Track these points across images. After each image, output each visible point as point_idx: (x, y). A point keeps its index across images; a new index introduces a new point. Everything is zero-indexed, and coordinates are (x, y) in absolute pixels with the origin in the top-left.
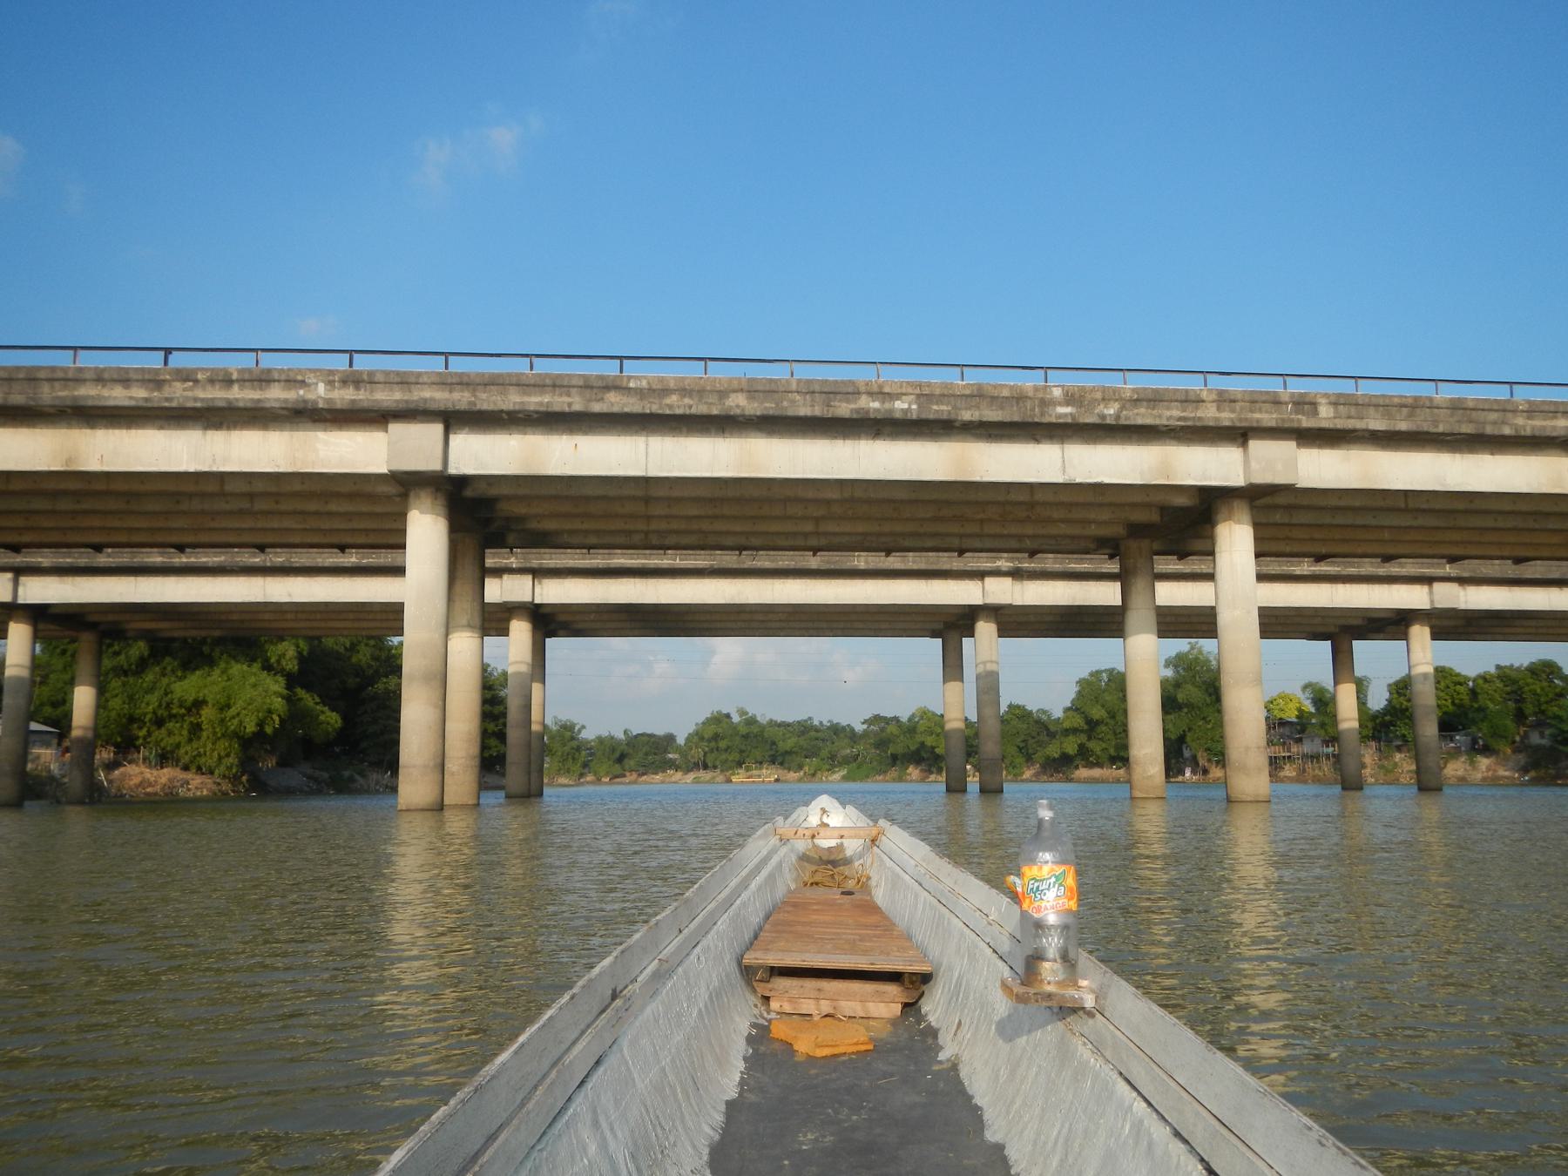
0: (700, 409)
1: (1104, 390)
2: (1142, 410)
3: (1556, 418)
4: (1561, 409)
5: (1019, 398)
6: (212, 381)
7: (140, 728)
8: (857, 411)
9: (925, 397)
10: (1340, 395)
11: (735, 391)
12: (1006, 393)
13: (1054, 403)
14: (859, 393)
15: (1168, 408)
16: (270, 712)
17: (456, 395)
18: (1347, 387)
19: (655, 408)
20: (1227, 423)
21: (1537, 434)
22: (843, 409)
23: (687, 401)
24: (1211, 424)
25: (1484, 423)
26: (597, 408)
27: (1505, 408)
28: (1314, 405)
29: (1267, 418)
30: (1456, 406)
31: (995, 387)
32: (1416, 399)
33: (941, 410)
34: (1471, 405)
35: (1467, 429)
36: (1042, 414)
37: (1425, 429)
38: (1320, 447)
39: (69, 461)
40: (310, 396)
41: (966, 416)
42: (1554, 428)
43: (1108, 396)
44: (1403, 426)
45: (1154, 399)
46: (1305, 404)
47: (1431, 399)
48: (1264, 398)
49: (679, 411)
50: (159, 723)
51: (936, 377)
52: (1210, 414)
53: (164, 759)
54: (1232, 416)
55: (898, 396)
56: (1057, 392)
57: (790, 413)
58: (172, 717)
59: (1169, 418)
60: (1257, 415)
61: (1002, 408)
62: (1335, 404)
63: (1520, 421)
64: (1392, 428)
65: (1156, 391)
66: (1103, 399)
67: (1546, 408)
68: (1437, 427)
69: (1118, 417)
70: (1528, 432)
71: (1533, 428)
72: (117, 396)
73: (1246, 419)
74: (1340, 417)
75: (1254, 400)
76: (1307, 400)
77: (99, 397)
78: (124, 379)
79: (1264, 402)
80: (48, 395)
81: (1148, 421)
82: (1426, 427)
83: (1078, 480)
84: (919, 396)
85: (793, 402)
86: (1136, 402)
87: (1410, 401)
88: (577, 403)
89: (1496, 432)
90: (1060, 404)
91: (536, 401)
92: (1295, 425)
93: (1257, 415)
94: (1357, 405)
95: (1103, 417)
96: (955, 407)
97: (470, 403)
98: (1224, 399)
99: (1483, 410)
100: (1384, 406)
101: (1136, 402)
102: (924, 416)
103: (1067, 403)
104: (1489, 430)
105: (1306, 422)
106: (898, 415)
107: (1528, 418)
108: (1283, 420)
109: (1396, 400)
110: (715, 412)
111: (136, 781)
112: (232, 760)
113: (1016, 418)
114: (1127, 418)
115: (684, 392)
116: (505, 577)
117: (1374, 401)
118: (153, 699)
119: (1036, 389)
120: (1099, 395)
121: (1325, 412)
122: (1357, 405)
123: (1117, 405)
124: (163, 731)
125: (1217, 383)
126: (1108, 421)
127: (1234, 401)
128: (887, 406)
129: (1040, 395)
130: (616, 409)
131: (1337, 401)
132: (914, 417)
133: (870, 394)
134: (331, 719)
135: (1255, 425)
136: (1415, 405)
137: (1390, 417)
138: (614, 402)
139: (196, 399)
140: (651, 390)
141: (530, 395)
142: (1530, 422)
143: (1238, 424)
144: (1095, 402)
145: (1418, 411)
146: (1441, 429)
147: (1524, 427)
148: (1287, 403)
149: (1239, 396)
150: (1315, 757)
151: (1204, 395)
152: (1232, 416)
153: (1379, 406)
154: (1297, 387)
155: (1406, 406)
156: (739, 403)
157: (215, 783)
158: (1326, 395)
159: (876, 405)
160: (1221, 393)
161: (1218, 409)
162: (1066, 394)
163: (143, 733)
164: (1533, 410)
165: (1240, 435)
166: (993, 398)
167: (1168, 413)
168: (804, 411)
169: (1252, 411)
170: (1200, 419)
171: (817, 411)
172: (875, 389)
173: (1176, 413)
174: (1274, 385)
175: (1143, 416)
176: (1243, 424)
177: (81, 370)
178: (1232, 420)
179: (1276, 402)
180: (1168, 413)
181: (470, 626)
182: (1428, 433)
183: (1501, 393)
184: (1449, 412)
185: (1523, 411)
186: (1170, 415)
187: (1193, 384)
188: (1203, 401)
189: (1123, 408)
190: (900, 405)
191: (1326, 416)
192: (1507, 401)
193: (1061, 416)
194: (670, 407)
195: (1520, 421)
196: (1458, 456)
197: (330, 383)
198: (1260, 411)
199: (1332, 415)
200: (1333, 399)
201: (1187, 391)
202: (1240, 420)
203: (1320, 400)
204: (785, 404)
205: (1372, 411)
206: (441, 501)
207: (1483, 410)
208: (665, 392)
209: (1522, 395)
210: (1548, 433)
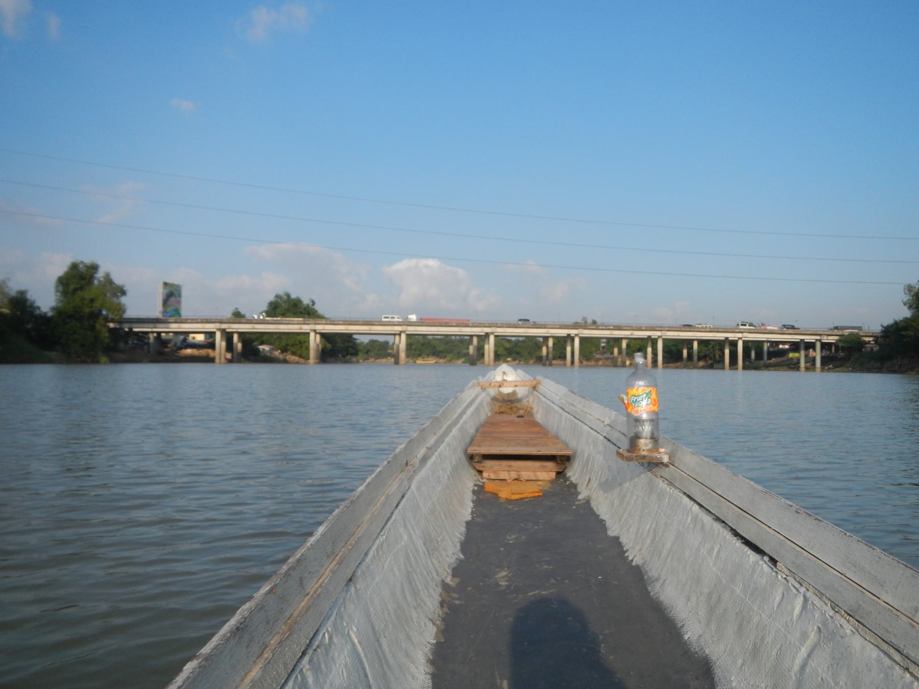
22: (448, 325)
29: (492, 325)
43: (475, 323)
45: (480, 324)
46: (497, 324)
50: (293, 345)
52: (487, 325)
53: (294, 354)
58: (296, 344)
72: (376, 323)
78: (377, 322)
98: (488, 323)
124: (292, 348)
134: (329, 346)
138: (425, 324)
150: (607, 359)
165: (490, 327)
186: (482, 325)
187: (484, 322)
191: (499, 325)
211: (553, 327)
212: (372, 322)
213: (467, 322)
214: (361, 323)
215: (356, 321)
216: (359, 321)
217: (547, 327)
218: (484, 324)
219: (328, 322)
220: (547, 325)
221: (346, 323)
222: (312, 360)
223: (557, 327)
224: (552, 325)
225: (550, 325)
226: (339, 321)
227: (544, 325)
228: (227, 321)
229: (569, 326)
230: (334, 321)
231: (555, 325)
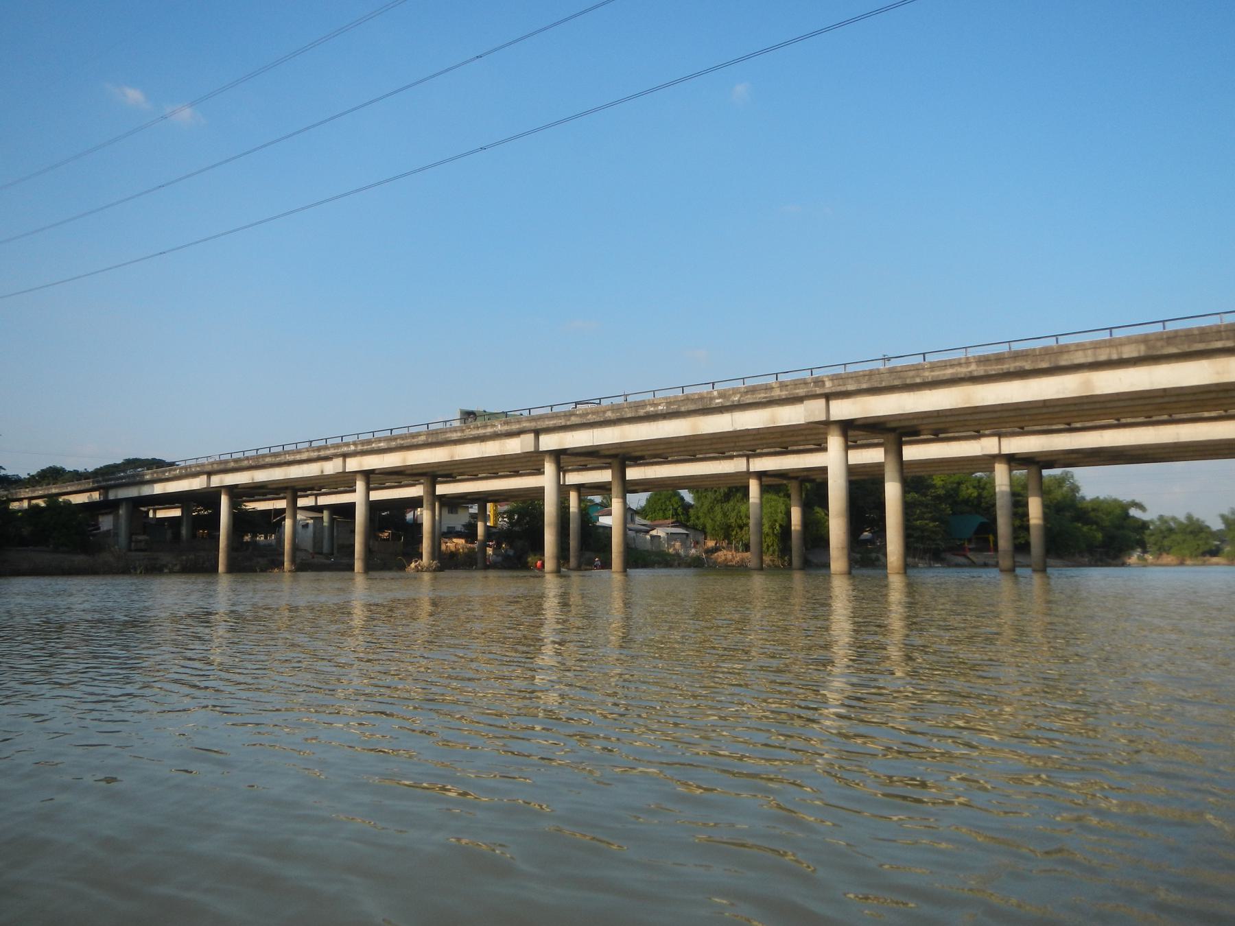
0: (598, 419)
1: (733, 389)
2: (749, 396)
3: (946, 369)
4: (948, 364)
5: (701, 398)
6: (474, 428)
7: (733, 531)
8: (645, 413)
9: (669, 404)
10: (834, 375)
11: (608, 410)
12: (696, 397)
13: (715, 398)
14: (646, 405)
15: (760, 394)
16: (776, 521)
17: (532, 424)
18: (841, 370)
19: (585, 421)
20: (784, 397)
21: (935, 379)
22: (642, 412)
23: (594, 416)
24: (777, 398)
25: (907, 378)
26: (568, 423)
27: (917, 368)
28: (823, 382)
29: (801, 391)
30: (892, 371)
31: (692, 394)
32: (871, 371)
33: (674, 407)
34: (899, 369)
35: (897, 382)
36: (710, 404)
37: (876, 386)
38: (842, 399)
39: (452, 457)
40: (497, 430)
41: (683, 409)
42: (944, 374)
43: (735, 391)
44: (864, 386)
45: (753, 390)
46: (819, 382)
47: (878, 369)
48: (799, 382)
49: (592, 421)
50: (741, 528)
51: (670, 394)
52: (777, 393)
54: (787, 393)
55: (659, 404)
56: (715, 393)
57: (625, 416)
59: (760, 398)
60: (797, 391)
61: (695, 404)
62: (832, 380)
63: (927, 374)
64: (858, 388)
65: (754, 386)
66: (733, 394)
67: (939, 364)
68: (882, 384)
69: (739, 401)
70: (930, 379)
71: (933, 376)
73: (793, 394)
74: (835, 386)
75: (796, 384)
76: (820, 379)
77: (451, 437)
79: (800, 384)
80: (441, 437)
81: (751, 401)
82: (876, 385)
83: (738, 429)
84: (667, 403)
85: (626, 412)
86: (747, 393)
87: (867, 373)
88: (562, 422)
89: (912, 382)
90: (717, 399)
91: (551, 423)
92: (814, 393)
93: (797, 391)
94: (842, 378)
95: (733, 402)
96: (679, 406)
97: (535, 427)
98: (783, 386)
99: (906, 371)
100: (855, 377)
101: (747, 393)
102: (670, 411)
103: (719, 398)
104: (908, 381)
105: (819, 391)
106: (659, 412)
107: (931, 371)
108: (808, 392)
109: (861, 373)
110: (602, 420)
111: (723, 558)
112: (775, 547)
113: (701, 407)
114: (743, 401)
115: (593, 413)
116: (735, 459)
117: (850, 375)
118: (734, 514)
119: (708, 393)
120: (731, 392)
121: (828, 384)
122: (842, 378)
123: (739, 396)
125: (782, 378)
126: (735, 403)
127: (787, 386)
128: (656, 409)
129: (709, 396)
130: (573, 423)
131: (834, 378)
132: (665, 412)
133: (650, 405)
135: (796, 396)
136: (871, 374)
137: (859, 382)
138: (574, 420)
139: (472, 435)
140: (583, 414)
141: (551, 421)
142: (932, 373)
143: (789, 397)
144: (730, 395)
145: (873, 377)
146: (884, 384)
147: (928, 377)
148: (811, 383)
149: (789, 383)
151: (774, 385)
152: (787, 393)
153: (852, 378)
154: (817, 374)
155: (865, 376)
156: (609, 415)
157: (771, 560)
158: (828, 376)
159: (652, 409)
160: (781, 383)
161: (781, 391)
162: (719, 394)
163: (734, 533)
164: (933, 367)
166: (693, 400)
167: (760, 396)
168: (629, 415)
169: (795, 389)
170: (773, 396)
171: (633, 415)
172: (651, 402)
173: (763, 395)
174: (806, 375)
175: (750, 399)
176: (792, 396)
177: (446, 428)
178: (786, 395)
179: (805, 383)
180: (760, 396)
181: (616, 497)
182: (877, 387)
183: (918, 360)
184: (888, 374)
185: (927, 368)
186: (760, 396)
187: (771, 380)
188: (773, 388)
189: (741, 396)
190: (660, 408)
191: (829, 386)
192: (919, 364)
193: (719, 403)
194: (589, 420)
195: (927, 374)
196: (912, 393)
197: (501, 424)
198: (799, 389)
199: (831, 385)
200: (830, 378)
201: (766, 384)
202: (789, 394)
203: (826, 379)
204: (623, 413)
205: (850, 381)
206: (553, 458)
207: (906, 371)
208: (587, 414)
209: (930, 358)
210: (941, 378)
211: (1103, 357)
212: (444, 432)
213: (705, 390)
214: (422, 439)
215: (413, 436)
216: (418, 434)
217: (1064, 361)
218: (768, 388)
219: (359, 448)
220: (1064, 350)
221: (393, 444)
222: (358, 565)
223: (1129, 352)
224: (1097, 346)
225: (1081, 347)
226: (380, 440)
227: (1046, 352)
228: (209, 468)
229: (1204, 334)
230: (369, 442)
231: (1110, 344)
